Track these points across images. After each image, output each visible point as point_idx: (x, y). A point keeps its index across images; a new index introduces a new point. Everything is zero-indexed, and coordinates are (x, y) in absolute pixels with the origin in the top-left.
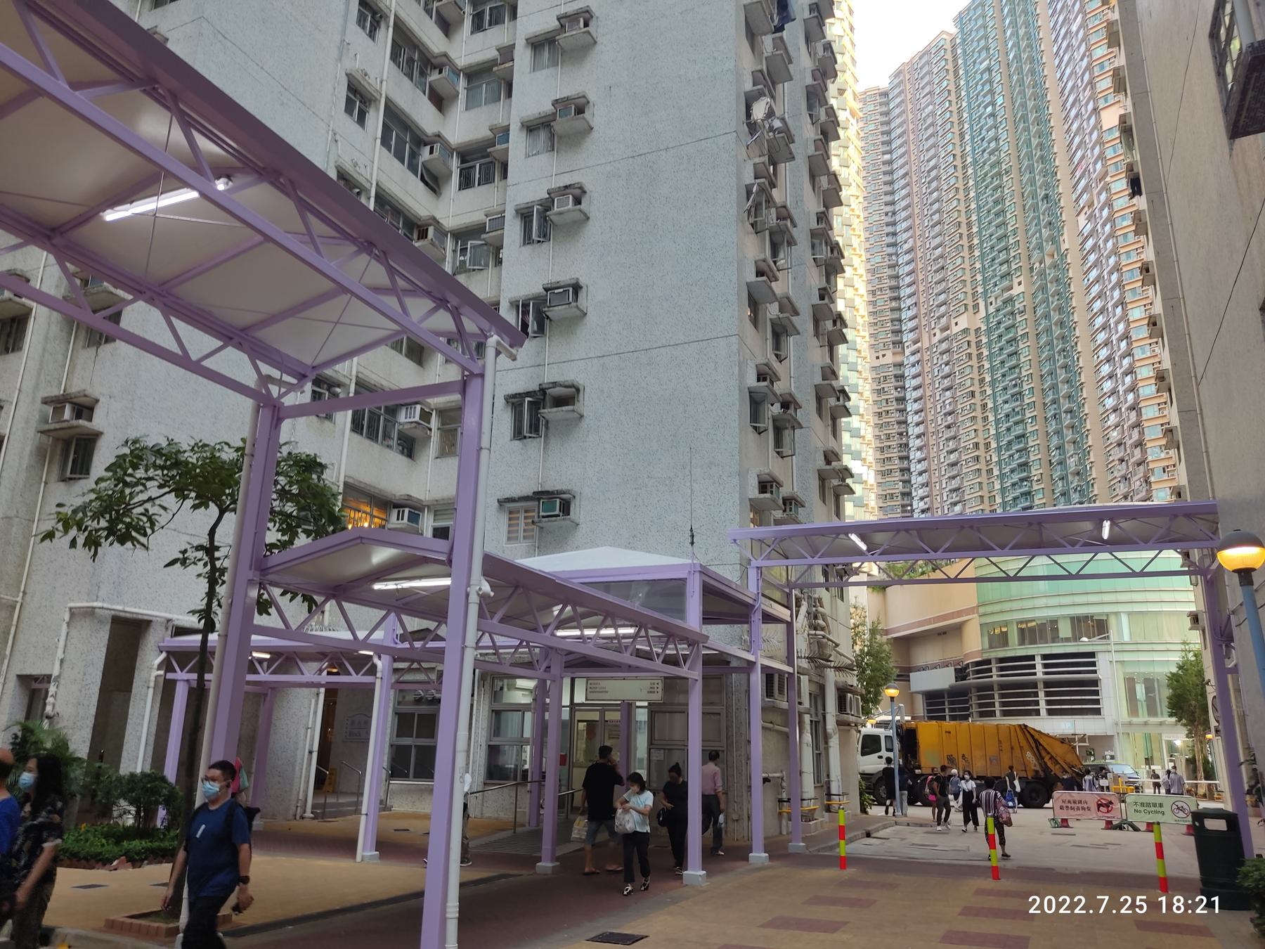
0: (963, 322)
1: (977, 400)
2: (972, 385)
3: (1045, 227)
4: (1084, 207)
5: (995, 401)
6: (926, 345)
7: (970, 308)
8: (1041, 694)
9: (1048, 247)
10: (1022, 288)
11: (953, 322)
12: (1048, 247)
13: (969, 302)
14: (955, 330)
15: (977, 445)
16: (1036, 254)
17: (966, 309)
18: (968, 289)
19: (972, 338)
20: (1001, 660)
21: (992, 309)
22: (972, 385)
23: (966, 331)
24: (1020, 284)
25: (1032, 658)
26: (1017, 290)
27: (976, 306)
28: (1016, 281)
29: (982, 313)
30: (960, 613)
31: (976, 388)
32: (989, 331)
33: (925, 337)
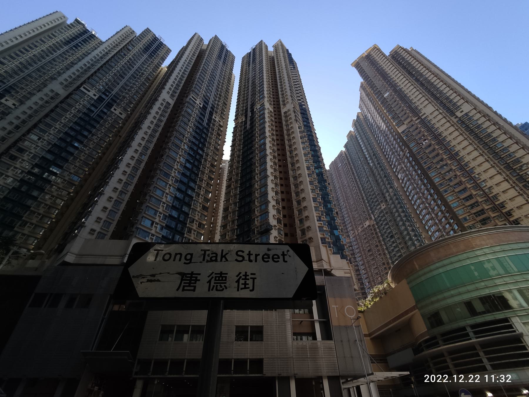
0: (367, 223)
1: (379, 247)
2: (376, 243)
3: (388, 185)
4: (399, 171)
5: (386, 246)
6: (357, 234)
7: (369, 219)
8: (481, 354)
9: (391, 190)
10: (385, 206)
11: (364, 224)
12: (391, 190)
13: (367, 217)
14: (365, 226)
15: (384, 264)
16: (387, 195)
17: (367, 219)
18: (366, 213)
19: (372, 228)
20: (443, 335)
21: (376, 216)
22: (376, 243)
23: (369, 226)
24: (383, 205)
25: (464, 329)
26: (383, 208)
27: (371, 218)
28: (382, 205)
29: (373, 218)
30: (407, 312)
31: (378, 244)
32: (377, 223)
33: (356, 231)
